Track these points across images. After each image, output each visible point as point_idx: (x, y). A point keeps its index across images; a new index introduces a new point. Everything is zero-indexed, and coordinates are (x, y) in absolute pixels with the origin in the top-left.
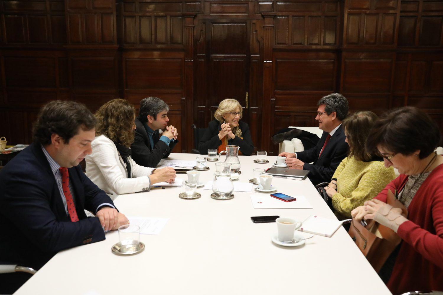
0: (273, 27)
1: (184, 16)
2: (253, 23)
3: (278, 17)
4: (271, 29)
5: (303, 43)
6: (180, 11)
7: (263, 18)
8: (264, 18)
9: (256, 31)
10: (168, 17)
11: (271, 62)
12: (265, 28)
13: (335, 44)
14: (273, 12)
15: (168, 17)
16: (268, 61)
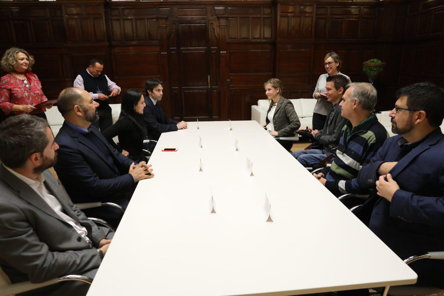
0: (226, 26)
1: (157, 18)
2: (211, 23)
3: (229, 19)
4: (225, 28)
5: (248, 38)
6: (154, 15)
7: (217, 19)
8: (219, 19)
9: (214, 29)
10: (146, 20)
11: (226, 52)
12: (220, 27)
13: (271, 38)
14: (226, 14)
15: (146, 20)
16: (224, 52)
